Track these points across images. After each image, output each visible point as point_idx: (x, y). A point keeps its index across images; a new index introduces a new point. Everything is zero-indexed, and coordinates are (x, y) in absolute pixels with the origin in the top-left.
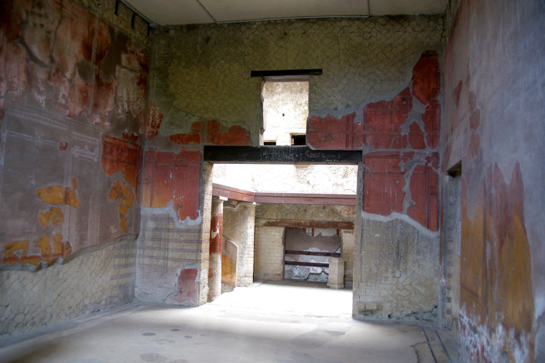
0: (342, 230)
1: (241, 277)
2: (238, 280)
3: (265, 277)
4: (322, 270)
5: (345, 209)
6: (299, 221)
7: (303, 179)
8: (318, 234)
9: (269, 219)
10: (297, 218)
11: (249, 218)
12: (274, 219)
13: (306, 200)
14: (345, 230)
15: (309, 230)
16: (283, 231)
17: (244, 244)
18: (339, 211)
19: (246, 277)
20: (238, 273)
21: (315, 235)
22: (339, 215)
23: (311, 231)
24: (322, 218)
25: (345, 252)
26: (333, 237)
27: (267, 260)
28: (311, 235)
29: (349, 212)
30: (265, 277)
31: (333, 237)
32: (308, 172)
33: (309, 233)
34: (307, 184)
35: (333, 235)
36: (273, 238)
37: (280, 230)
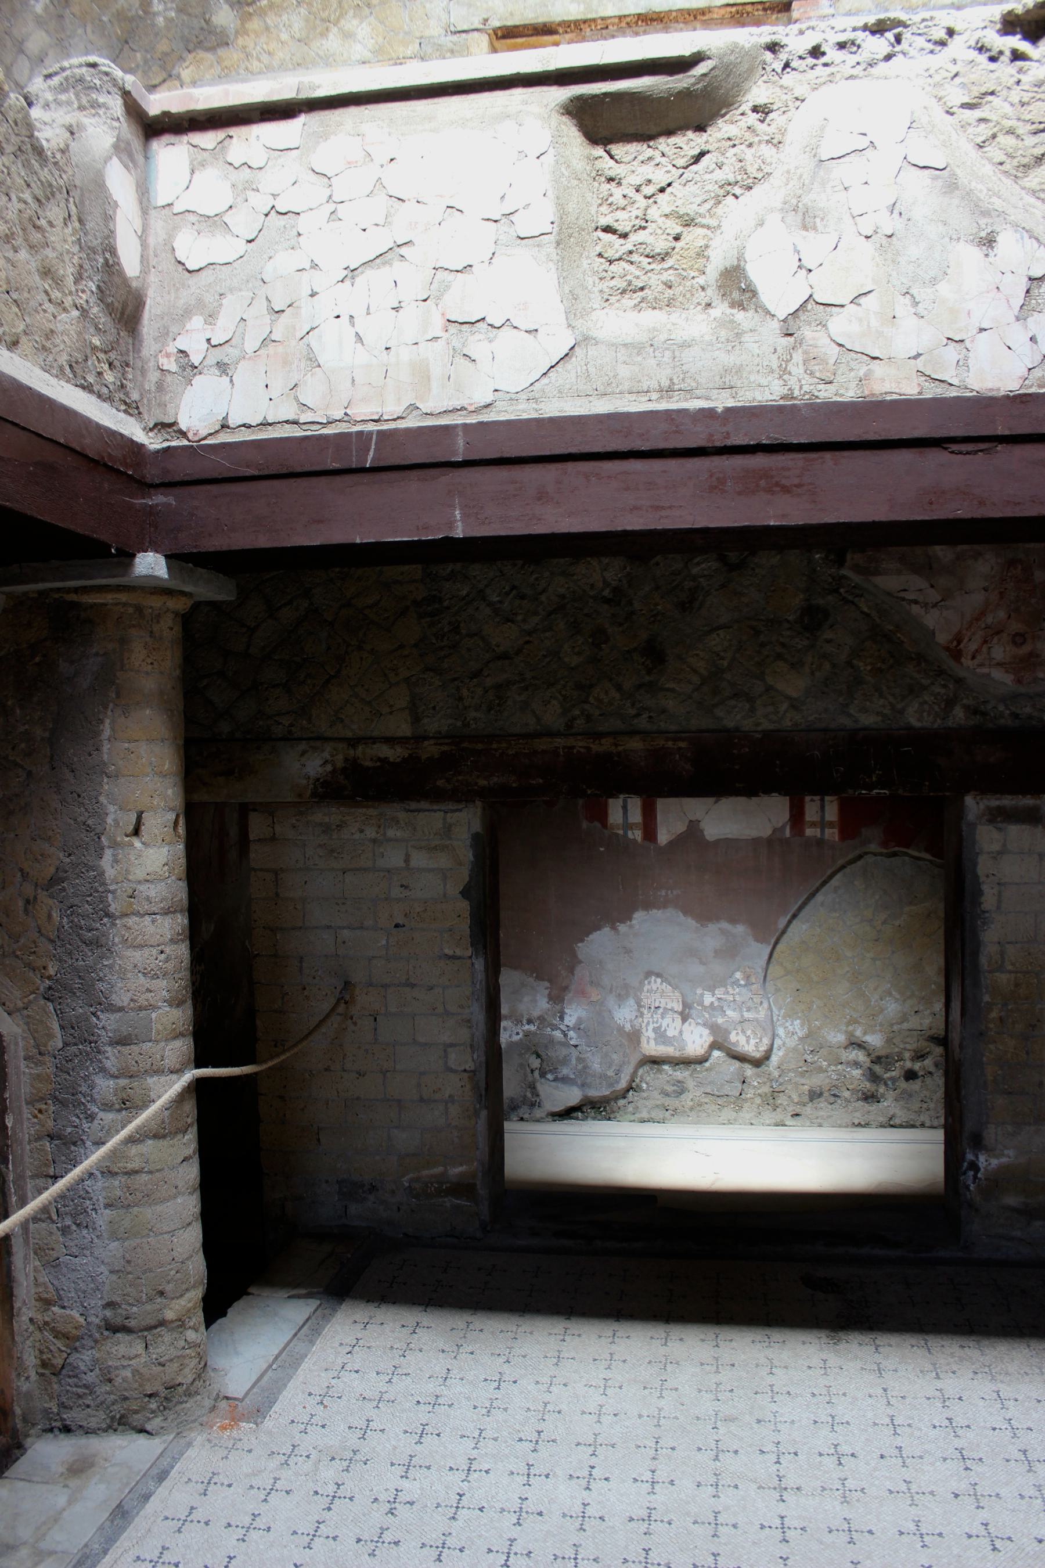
0: (973, 805)
1: (71, 1340)
2: (44, 1364)
3: (354, 1209)
4: (711, 1039)
5: (989, 619)
6: (605, 746)
7: (664, 257)
8: (681, 828)
9: (353, 742)
10: (589, 718)
11: (107, 732)
12: (389, 740)
13: (717, 486)
14: (994, 803)
15: (625, 808)
16: (476, 837)
17: (78, 1008)
18: (942, 638)
19: (128, 1330)
20: (46, 1303)
21: (663, 837)
22: (941, 672)
23: (636, 816)
24: (795, 705)
25: (1002, 978)
26: (772, 843)
27: (360, 1074)
28: (637, 835)
29: (1026, 649)
30: (354, 1209)
31: (769, 842)
32: (720, 175)
33: (628, 826)
34: (721, 309)
35: (766, 832)
36: (396, 892)
37: (448, 829)
